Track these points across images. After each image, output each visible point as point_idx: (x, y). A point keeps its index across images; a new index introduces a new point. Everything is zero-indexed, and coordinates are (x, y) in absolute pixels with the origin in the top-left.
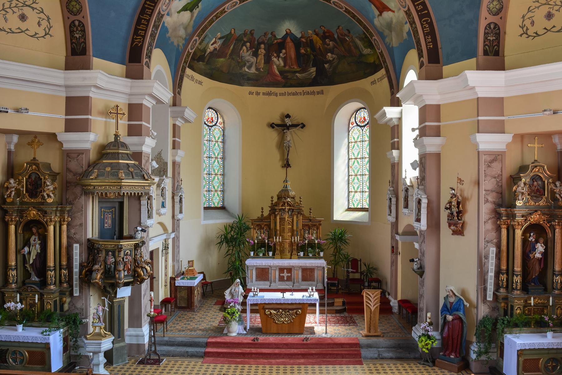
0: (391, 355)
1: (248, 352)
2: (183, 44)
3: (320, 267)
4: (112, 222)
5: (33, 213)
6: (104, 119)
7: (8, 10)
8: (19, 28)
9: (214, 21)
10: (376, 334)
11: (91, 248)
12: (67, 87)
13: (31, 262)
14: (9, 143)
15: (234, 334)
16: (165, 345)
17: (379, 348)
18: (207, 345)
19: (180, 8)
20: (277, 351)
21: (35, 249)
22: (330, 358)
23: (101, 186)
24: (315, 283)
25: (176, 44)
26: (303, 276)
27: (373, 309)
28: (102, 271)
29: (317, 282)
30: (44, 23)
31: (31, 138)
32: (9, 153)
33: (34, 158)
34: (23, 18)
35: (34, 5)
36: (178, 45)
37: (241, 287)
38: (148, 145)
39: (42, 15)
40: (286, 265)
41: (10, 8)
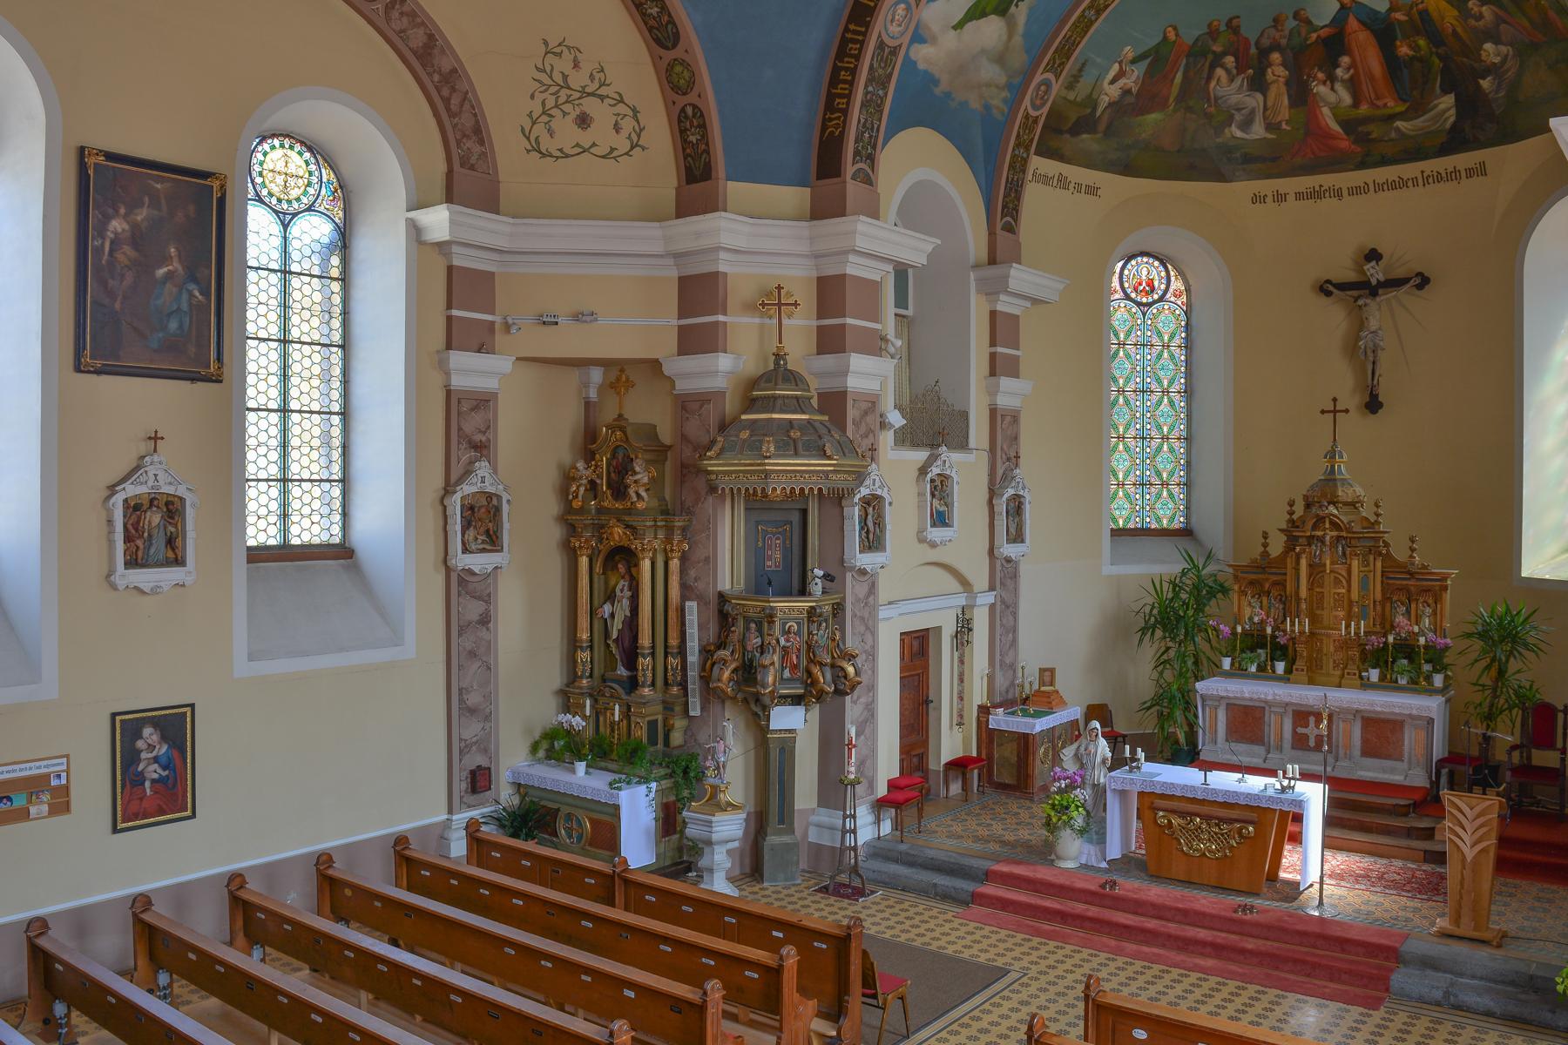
0: (1486, 1002)
1: (1077, 911)
2: (1005, 101)
3: (1420, 718)
4: (784, 557)
5: (618, 533)
6: (757, 320)
7: (554, 112)
8: (578, 145)
9: (1092, 23)
10: (1476, 935)
11: (723, 612)
12: (677, 256)
13: (615, 636)
14: (586, 385)
15: (1070, 865)
16: (896, 861)
17: (1461, 975)
18: (989, 876)
19: (960, 16)
20: (1152, 924)
21: (622, 609)
22: (1292, 972)
23: (729, 473)
24: (1405, 765)
25: (975, 104)
26: (1365, 741)
27: (1470, 854)
28: (733, 666)
29: (1410, 762)
30: (628, 125)
31: (620, 374)
32: (588, 404)
33: (620, 416)
34: (583, 121)
35: (603, 91)
36: (987, 107)
37: (1103, 742)
38: (868, 374)
39: (621, 108)
40: (1311, 702)
41: (556, 106)
